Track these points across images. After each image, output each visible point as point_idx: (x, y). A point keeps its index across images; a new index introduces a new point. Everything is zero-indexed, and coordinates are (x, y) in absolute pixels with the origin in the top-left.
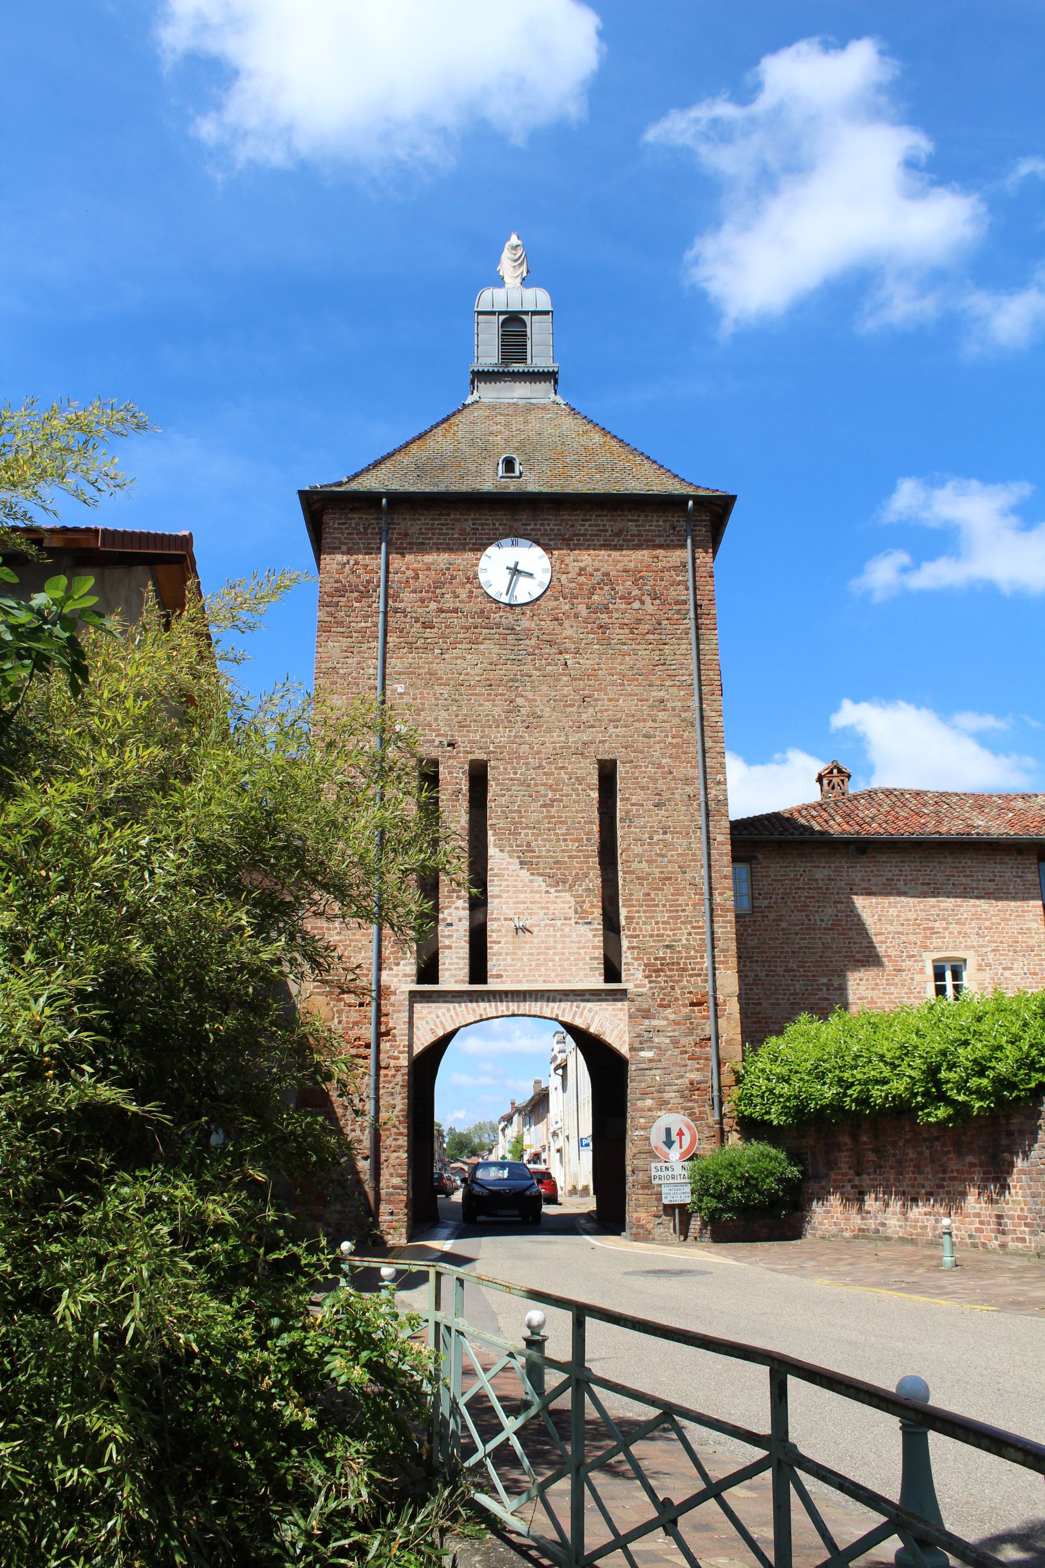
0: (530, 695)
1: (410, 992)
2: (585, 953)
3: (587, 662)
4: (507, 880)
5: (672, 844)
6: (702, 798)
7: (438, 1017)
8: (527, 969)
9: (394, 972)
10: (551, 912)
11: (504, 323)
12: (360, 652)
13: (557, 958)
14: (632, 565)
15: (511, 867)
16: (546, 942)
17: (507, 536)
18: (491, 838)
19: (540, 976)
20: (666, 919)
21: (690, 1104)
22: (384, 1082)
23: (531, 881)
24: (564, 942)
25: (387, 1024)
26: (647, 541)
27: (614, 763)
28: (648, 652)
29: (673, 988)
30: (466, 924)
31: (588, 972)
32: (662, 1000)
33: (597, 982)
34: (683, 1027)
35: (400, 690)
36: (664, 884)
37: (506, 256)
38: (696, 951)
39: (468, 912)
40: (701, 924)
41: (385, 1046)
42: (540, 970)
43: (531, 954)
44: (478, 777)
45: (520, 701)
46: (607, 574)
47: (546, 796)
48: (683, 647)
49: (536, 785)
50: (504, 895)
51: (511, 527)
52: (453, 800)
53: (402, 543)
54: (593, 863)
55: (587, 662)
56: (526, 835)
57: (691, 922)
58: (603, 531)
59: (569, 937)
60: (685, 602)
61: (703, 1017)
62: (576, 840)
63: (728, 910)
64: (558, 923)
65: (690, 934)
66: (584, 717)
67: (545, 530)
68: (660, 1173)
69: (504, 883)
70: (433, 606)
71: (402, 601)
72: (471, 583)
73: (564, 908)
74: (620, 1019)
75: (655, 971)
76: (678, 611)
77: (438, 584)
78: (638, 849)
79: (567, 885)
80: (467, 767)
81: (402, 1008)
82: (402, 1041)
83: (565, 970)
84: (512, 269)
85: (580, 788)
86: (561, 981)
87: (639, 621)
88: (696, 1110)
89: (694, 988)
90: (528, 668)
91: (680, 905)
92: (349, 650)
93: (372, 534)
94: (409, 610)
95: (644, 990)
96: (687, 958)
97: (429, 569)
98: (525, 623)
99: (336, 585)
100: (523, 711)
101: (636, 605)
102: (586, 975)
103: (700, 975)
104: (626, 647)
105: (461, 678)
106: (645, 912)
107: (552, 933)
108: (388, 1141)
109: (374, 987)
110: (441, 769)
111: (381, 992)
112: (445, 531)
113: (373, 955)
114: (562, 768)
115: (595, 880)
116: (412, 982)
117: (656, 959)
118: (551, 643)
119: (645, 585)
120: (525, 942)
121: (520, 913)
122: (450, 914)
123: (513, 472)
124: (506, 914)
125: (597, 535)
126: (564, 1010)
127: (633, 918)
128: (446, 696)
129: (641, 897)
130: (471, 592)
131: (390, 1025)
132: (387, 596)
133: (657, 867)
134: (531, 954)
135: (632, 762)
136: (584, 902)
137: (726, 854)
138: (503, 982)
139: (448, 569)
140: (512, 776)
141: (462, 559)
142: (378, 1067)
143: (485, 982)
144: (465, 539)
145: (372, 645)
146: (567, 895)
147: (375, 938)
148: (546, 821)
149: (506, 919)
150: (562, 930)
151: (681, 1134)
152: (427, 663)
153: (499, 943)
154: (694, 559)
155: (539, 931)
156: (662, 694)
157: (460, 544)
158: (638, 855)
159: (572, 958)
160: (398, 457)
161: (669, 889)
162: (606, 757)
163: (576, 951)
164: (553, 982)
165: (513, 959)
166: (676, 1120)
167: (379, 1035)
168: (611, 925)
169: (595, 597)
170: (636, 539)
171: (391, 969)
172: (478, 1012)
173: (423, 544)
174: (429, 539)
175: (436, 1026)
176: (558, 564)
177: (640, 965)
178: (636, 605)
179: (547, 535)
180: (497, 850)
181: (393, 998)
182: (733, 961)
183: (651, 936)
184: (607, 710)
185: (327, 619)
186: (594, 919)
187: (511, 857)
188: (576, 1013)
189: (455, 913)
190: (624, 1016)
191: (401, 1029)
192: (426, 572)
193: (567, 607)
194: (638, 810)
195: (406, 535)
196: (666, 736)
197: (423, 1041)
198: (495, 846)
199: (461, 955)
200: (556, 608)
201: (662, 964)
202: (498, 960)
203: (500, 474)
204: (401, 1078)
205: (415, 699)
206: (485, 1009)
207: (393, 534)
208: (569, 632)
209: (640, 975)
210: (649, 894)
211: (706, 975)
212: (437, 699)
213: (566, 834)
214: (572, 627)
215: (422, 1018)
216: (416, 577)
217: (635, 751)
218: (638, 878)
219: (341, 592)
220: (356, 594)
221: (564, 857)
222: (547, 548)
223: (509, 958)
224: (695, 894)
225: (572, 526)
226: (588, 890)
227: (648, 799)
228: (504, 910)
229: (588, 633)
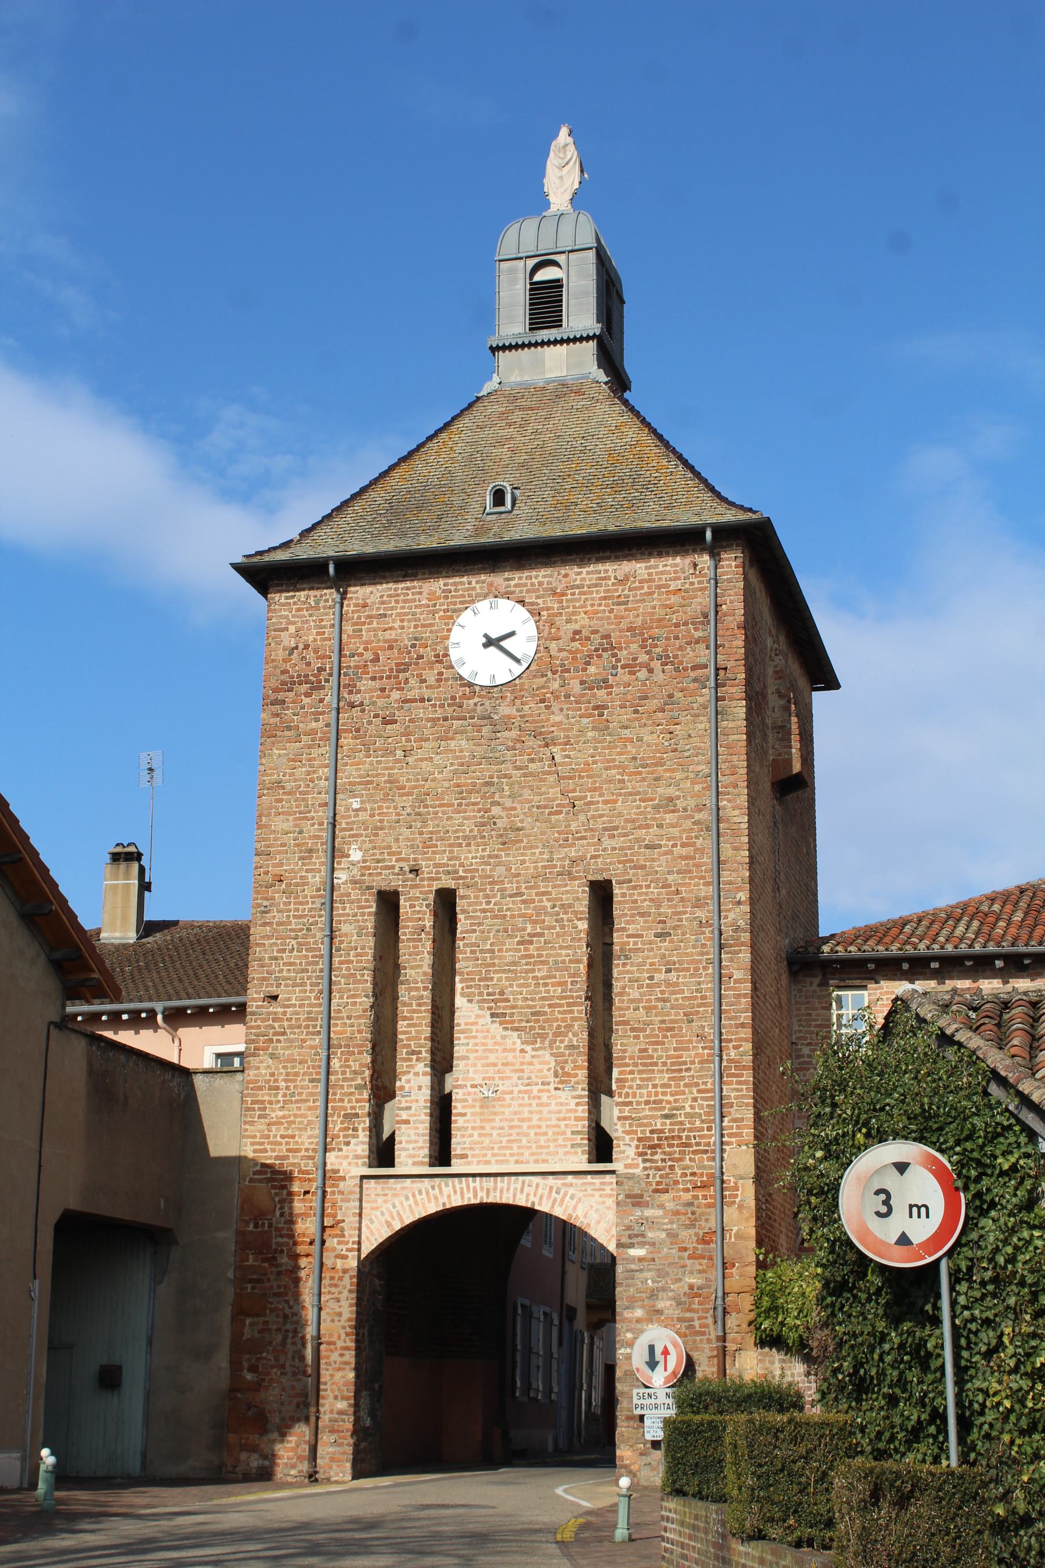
0: (509, 804)
1: (363, 1177)
2: (566, 1126)
3: (580, 756)
4: (476, 1037)
5: (677, 984)
6: (716, 925)
7: (394, 1207)
8: (496, 1146)
9: (344, 1153)
10: (526, 1075)
12: (309, 760)
13: (532, 1132)
14: (639, 622)
15: (481, 1021)
16: (520, 1113)
17: (485, 596)
18: (458, 986)
19: (511, 1155)
20: (665, 1081)
21: (688, 1315)
22: (331, 1285)
23: (504, 1037)
24: (541, 1112)
25: (334, 1216)
26: (659, 587)
27: (610, 881)
28: (655, 735)
29: (672, 1168)
30: (426, 1093)
31: (568, 1149)
32: (658, 1183)
34: (683, 1217)
35: (356, 806)
36: (666, 1037)
38: (703, 1121)
39: (429, 1077)
40: (709, 1086)
41: (331, 1242)
42: (511, 1148)
43: (502, 1128)
45: (496, 810)
46: (607, 637)
47: (524, 929)
48: (702, 726)
49: (513, 916)
50: (472, 1056)
51: (491, 585)
52: (414, 940)
53: (359, 618)
54: (580, 1012)
55: (580, 756)
56: (500, 979)
57: (697, 1084)
58: (605, 578)
59: (548, 1105)
60: (705, 666)
61: (709, 1206)
62: (560, 984)
63: (744, 1068)
64: (535, 1088)
65: (695, 1099)
66: (574, 827)
67: (532, 584)
68: (642, 1401)
69: (471, 1042)
70: (396, 695)
71: (359, 692)
72: (441, 662)
73: (541, 1071)
74: (608, 1208)
75: (651, 1147)
76: (695, 680)
79: (547, 1042)
80: (432, 896)
81: (352, 1197)
82: (351, 1235)
83: (541, 1147)
84: (557, 181)
85: (565, 917)
86: (536, 1162)
88: (697, 1323)
89: (698, 1168)
90: (507, 768)
91: (685, 1063)
92: (296, 759)
93: (324, 607)
94: (366, 702)
95: (637, 1171)
96: (690, 1130)
97: (391, 648)
98: (505, 710)
99: (283, 677)
100: (500, 824)
101: (643, 674)
102: (566, 1153)
103: (706, 1152)
104: (627, 731)
105: (428, 784)
106: (640, 1072)
107: (526, 1101)
109: (320, 1172)
110: (402, 902)
112: (410, 597)
113: (318, 1131)
114: (544, 894)
115: (580, 1037)
116: (364, 1164)
117: (652, 1132)
119: (656, 646)
120: (495, 1114)
121: (489, 1078)
122: (408, 1081)
123: (503, 505)
124: (473, 1079)
125: (596, 585)
126: (541, 1197)
127: (626, 1080)
128: (409, 810)
129: (637, 1054)
130: (440, 674)
131: (339, 1218)
133: (656, 1016)
134: (502, 1128)
135: (630, 881)
136: (566, 1062)
137: (745, 996)
138: (469, 1163)
139: (414, 646)
140: (484, 906)
143: (449, 1164)
144: (435, 605)
145: (322, 750)
146: (546, 1055)
147: (320, 1112)
148: (524, 961)
149: (473, 1086)
150: (539, 1098)
151: (666, 1352)
152: (387, 769)
153: (464, 1115)
155: (512, 1099)
156: (672, 791)
157: (429, 613)
158: (633, 1001)
159: (550, 1133)
160: (372, 494)
162: (600, 878)
163: (554, 1122)
164: (528, 1162)
165: (480, 1135)
166: (659, 1335)
169: (592, 669)
170: (646, 585)
171: (340, 1150)
172: (441, 1201)
173: (385, 616)
174: (392, 609)
175: (393, 1218)
176: (547, 629)
177: (632, 1139)
178: (643, 674)
179: (534, 591)
180: (465, 1000)
181: (342, 1184)
182: (748, 1133)
183: (647, 1103)
184: (601, 816)
185: (272, 721)
186: (578, 1083)
187: (481, 1008)
188: (555, 1200)
189: (414, 1083)
190: (611, 1202)
191: (351, 1222)
192: (388, 652)
193: (556, 685)
194: (635, 943)
195: (365, 606)
196: (674, 845)
197: (377, 1231)
198: (463, 995)
199: (421, 1131)
200: (543, 687)
201: (659, 1139)
202: (463, 1136)
203: (488, 510)
204: (348, 1283)
205: (372, 815)
206: (449, 1196)
207: (349, 605)
208: (557, 718)
209: (631, 1152)
210: (646, 1050)
211: (713, 1151)
212: (398, 814)
213: (548, 977)
214: (561, 710)
215: (377, 1208)
216: (376, 660)
217: (635, 867)
218: (633, 1030)
219: (288, 686)
220: (305, 687)
221: (543, 1006)
223: (476, 1133)
224: (703, 1048)
225: (566, 576)
226: (571, 1047)
227: (649, 928)
228: (471, 1075)
229: (581, 716)
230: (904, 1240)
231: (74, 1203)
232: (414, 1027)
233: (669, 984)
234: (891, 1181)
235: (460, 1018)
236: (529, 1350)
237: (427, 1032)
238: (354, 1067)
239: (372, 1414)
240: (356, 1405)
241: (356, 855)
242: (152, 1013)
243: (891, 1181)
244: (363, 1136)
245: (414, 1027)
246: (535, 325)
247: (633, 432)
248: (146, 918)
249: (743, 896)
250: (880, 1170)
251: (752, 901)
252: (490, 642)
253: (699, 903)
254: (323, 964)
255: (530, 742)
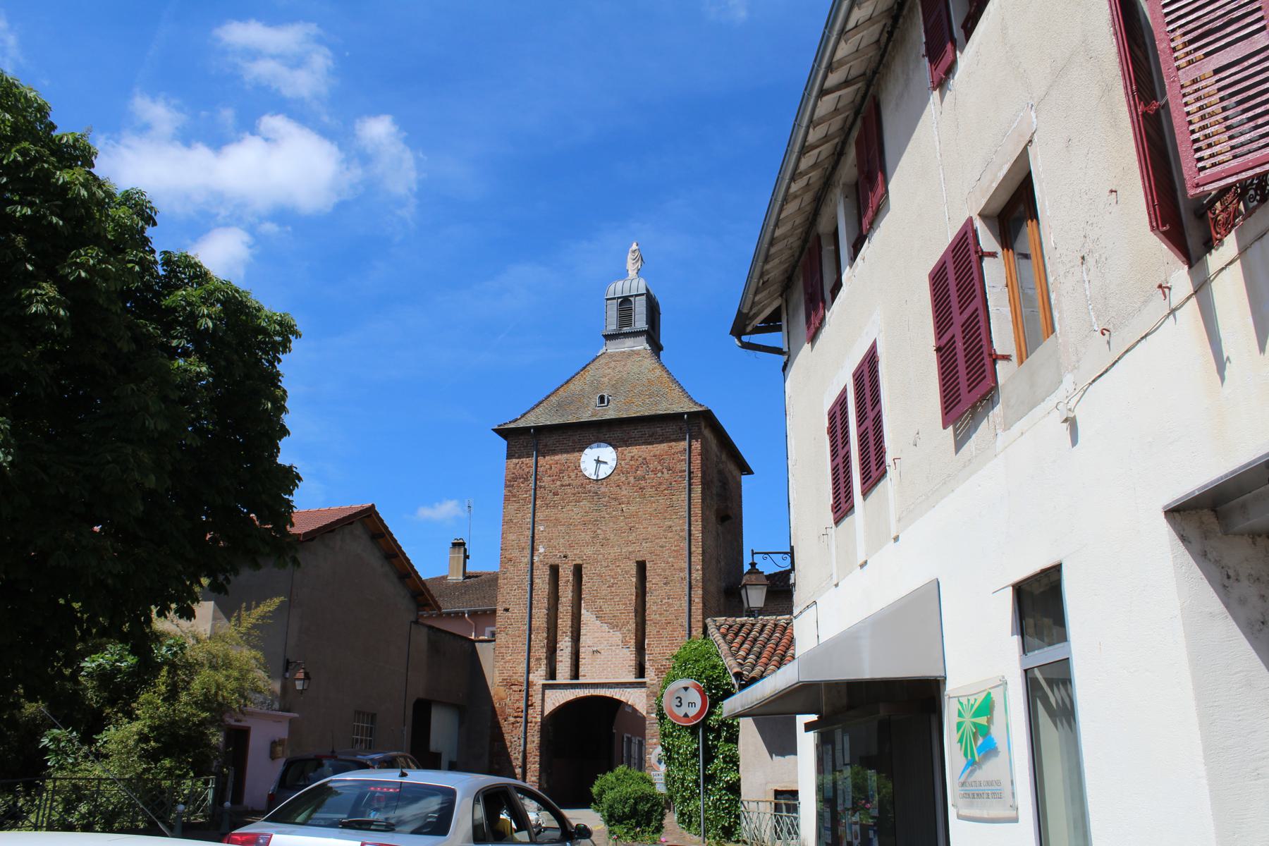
3: (633, 508)
11: (621, 304)
33: (632, 679)
37: (630, 256)
41: (530, 711)
44: (578, 571)
55: (633, 508)
70: (558, 483)
77: (561, 471)
78: (654, 608)
82: (538, 709)
87: (660, 484)
98: (603, 489)
108: (530, 759)
111: (529, 684)
118: (615, 499)
132: (536, 479)
141: (572, 457)
142: (527, 722)
154: (690, 446)
161: (669, 628)
167: (528, 706)
168: (640, 649)
189: (565, 644)
197: (549, 708)
204: (537, 728)
208: (624, 492)
219: (515, 479)
222: (615, 447)
230: (686, 715)
231: (422, 695)
232: (564, 622)
233: (669, 605)
234: (682, 694)
235: (583, 618)
236: (630, 756)
237: (569, 623)
238: (540, 640)
239: (547, 782)
240: (540, 779)
241: (541, 550)
242: (463, 613)
243: (682, 694)
244: (543, 667)
245: (564, 622)
246: (621, 326)
247: (658, 372)
248: (468, 570)
249: (699, 567)
250: (677, 690)
251: (703, 569)
252: (598, 461)
253: (681, 570)
254: (528, 596)
255: (614, 503)
